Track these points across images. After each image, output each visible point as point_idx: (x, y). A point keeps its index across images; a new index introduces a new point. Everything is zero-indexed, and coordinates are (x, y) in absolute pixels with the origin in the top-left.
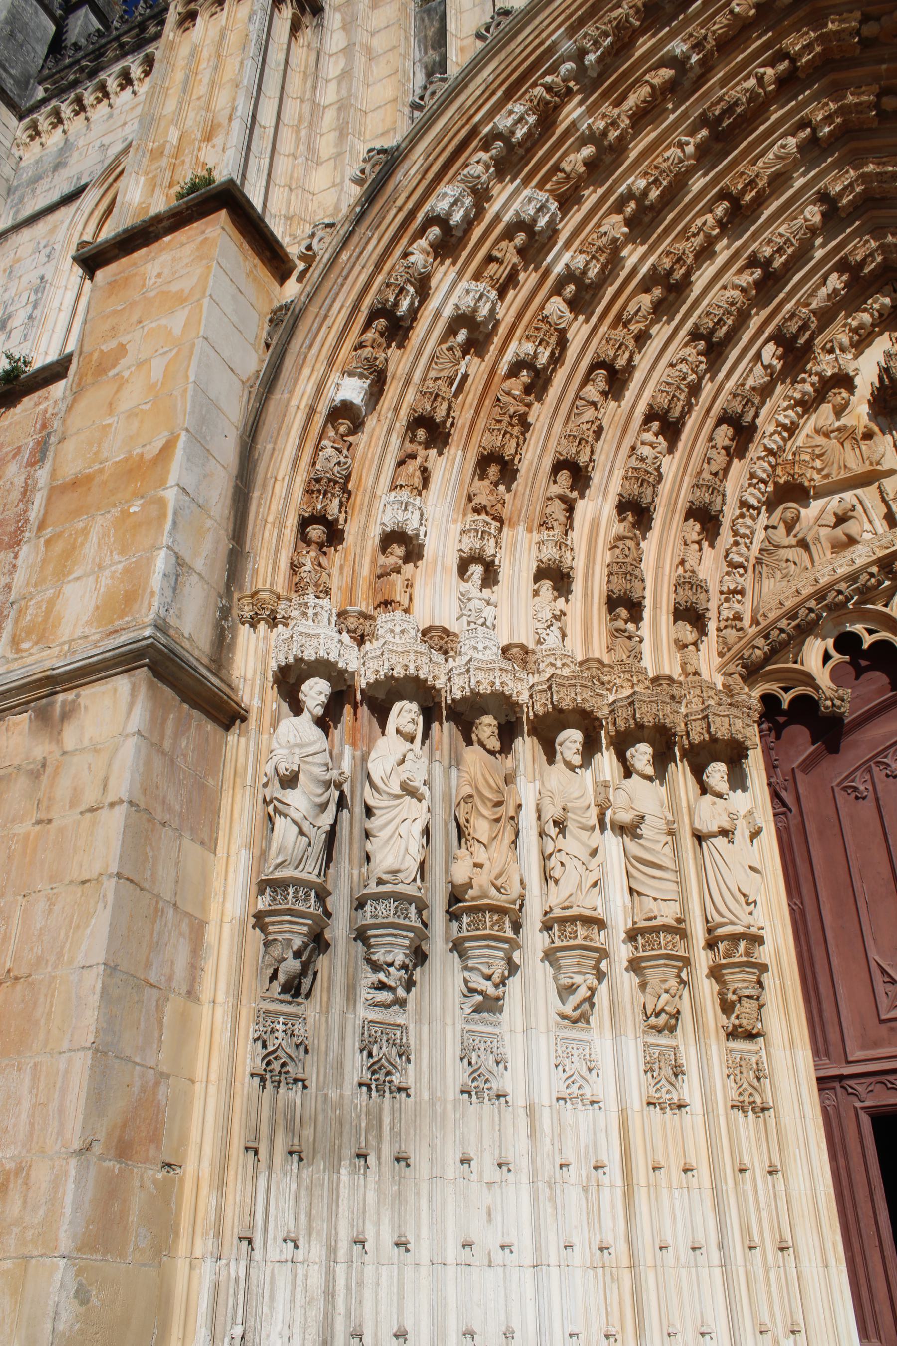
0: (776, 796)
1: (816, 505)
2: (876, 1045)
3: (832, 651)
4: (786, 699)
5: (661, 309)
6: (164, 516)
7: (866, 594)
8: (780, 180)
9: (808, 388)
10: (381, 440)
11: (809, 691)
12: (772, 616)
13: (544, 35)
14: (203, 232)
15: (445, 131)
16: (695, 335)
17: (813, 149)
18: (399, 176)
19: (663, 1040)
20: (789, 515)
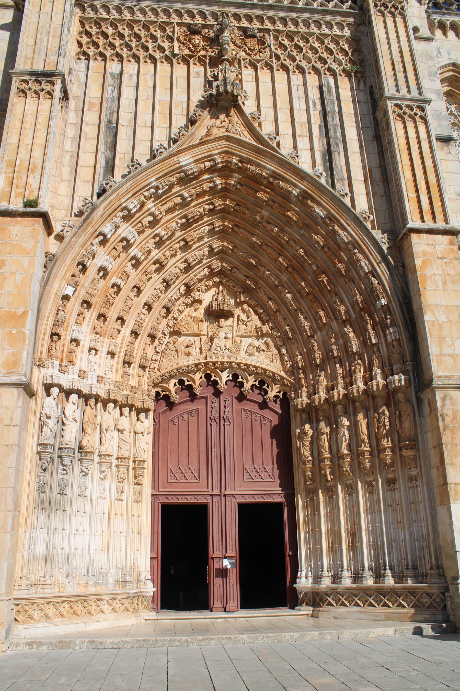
0: (154, 419)
1: (183, 338)
2: (166, 488)
3: (177, 384)
4: (162, 394)
5: (158, 271)
6: (24, 339)
7: (189, 372)
8: (200, 239)
9: (190, 301)
10: (74, 306)
11: (169, 394)
12: (165, 371)
13: (148, 177)
14: (34, 225)
15: (111, 201)
16: (164, 281)
17: (212, 232)
18: (94, 214)
19: (121, 484)
20: (175, 340)
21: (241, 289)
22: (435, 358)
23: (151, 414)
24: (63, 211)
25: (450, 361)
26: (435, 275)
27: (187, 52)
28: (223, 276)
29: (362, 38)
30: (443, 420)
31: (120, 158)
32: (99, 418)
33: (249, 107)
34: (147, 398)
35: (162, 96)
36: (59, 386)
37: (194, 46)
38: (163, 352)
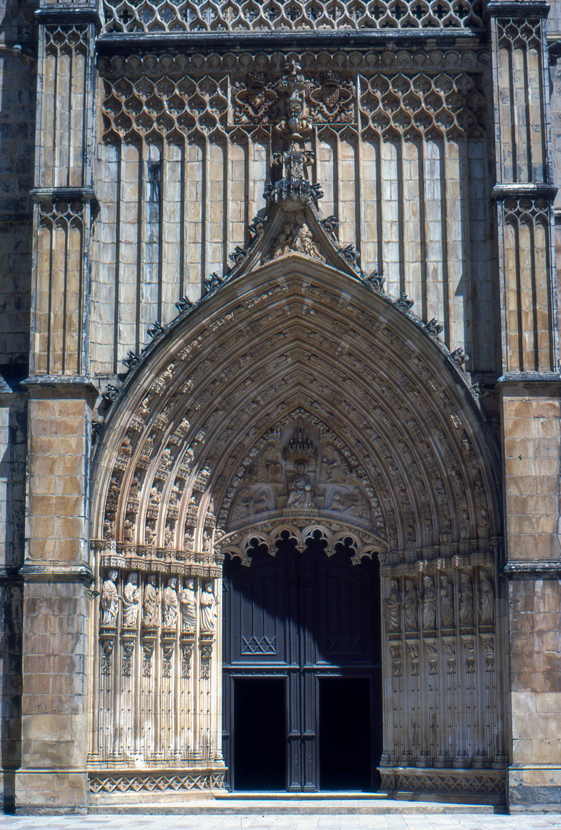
23: (219, 584)
32: (160, 596)
38: (231, 507)
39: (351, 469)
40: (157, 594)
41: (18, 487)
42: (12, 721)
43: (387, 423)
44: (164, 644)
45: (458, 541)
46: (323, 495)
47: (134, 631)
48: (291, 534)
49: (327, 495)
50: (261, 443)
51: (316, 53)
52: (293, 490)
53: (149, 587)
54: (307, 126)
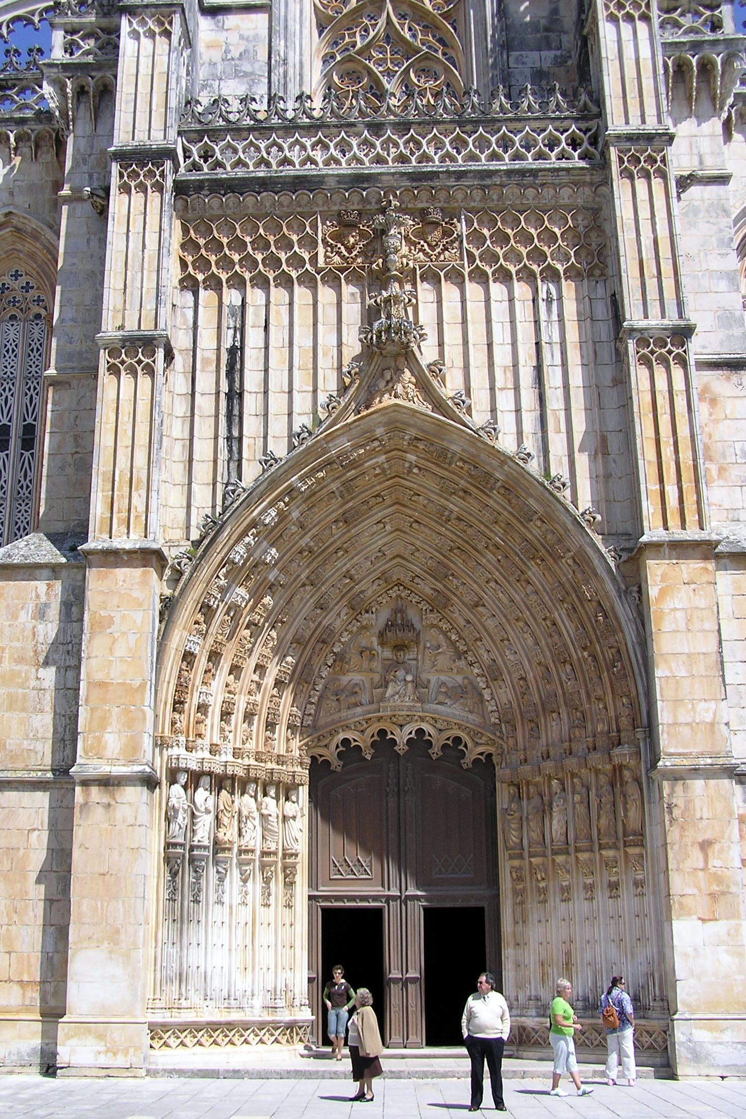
4: (321, 759)
21: (428, 606)
22: (665, 729)
24: (178, 530)
25: (686, 731)
26: (676, 609)
27: (337, 259)
28: (401, 588)
29: (604, 206)
30: (671, 813)
31: (249, 446)
32: (236, 804)
33: (427, 354)
34: (299, 769)
35: (303, 339)
36: (186, 770)
37: (347, 248)
39: (460, 655)
40: (233, 802)
41: (71, 674)
42: (57, 957)
43: (505, 600)
44: (240, 864)
45: (594, 736)
46: (427, 687)
47: (205, 848)
48: (389, 733)
49: (432, 685)
50: (354, 625)
51: (416, 188)
52: (392, 680)
53: (224, 793)
54: (408, 264)
